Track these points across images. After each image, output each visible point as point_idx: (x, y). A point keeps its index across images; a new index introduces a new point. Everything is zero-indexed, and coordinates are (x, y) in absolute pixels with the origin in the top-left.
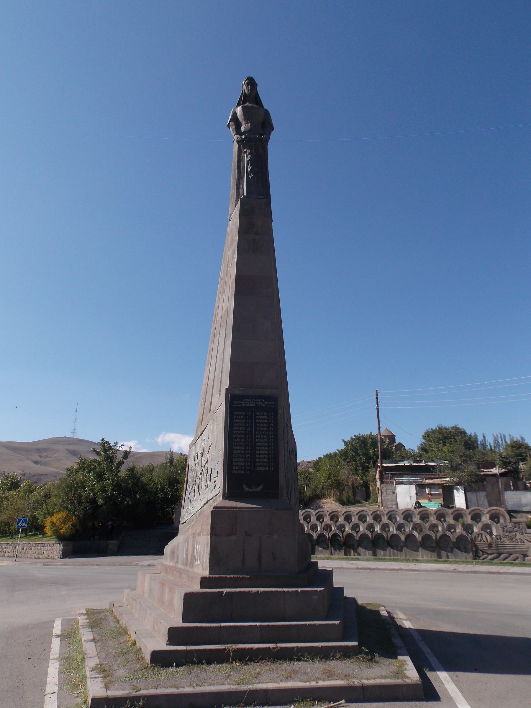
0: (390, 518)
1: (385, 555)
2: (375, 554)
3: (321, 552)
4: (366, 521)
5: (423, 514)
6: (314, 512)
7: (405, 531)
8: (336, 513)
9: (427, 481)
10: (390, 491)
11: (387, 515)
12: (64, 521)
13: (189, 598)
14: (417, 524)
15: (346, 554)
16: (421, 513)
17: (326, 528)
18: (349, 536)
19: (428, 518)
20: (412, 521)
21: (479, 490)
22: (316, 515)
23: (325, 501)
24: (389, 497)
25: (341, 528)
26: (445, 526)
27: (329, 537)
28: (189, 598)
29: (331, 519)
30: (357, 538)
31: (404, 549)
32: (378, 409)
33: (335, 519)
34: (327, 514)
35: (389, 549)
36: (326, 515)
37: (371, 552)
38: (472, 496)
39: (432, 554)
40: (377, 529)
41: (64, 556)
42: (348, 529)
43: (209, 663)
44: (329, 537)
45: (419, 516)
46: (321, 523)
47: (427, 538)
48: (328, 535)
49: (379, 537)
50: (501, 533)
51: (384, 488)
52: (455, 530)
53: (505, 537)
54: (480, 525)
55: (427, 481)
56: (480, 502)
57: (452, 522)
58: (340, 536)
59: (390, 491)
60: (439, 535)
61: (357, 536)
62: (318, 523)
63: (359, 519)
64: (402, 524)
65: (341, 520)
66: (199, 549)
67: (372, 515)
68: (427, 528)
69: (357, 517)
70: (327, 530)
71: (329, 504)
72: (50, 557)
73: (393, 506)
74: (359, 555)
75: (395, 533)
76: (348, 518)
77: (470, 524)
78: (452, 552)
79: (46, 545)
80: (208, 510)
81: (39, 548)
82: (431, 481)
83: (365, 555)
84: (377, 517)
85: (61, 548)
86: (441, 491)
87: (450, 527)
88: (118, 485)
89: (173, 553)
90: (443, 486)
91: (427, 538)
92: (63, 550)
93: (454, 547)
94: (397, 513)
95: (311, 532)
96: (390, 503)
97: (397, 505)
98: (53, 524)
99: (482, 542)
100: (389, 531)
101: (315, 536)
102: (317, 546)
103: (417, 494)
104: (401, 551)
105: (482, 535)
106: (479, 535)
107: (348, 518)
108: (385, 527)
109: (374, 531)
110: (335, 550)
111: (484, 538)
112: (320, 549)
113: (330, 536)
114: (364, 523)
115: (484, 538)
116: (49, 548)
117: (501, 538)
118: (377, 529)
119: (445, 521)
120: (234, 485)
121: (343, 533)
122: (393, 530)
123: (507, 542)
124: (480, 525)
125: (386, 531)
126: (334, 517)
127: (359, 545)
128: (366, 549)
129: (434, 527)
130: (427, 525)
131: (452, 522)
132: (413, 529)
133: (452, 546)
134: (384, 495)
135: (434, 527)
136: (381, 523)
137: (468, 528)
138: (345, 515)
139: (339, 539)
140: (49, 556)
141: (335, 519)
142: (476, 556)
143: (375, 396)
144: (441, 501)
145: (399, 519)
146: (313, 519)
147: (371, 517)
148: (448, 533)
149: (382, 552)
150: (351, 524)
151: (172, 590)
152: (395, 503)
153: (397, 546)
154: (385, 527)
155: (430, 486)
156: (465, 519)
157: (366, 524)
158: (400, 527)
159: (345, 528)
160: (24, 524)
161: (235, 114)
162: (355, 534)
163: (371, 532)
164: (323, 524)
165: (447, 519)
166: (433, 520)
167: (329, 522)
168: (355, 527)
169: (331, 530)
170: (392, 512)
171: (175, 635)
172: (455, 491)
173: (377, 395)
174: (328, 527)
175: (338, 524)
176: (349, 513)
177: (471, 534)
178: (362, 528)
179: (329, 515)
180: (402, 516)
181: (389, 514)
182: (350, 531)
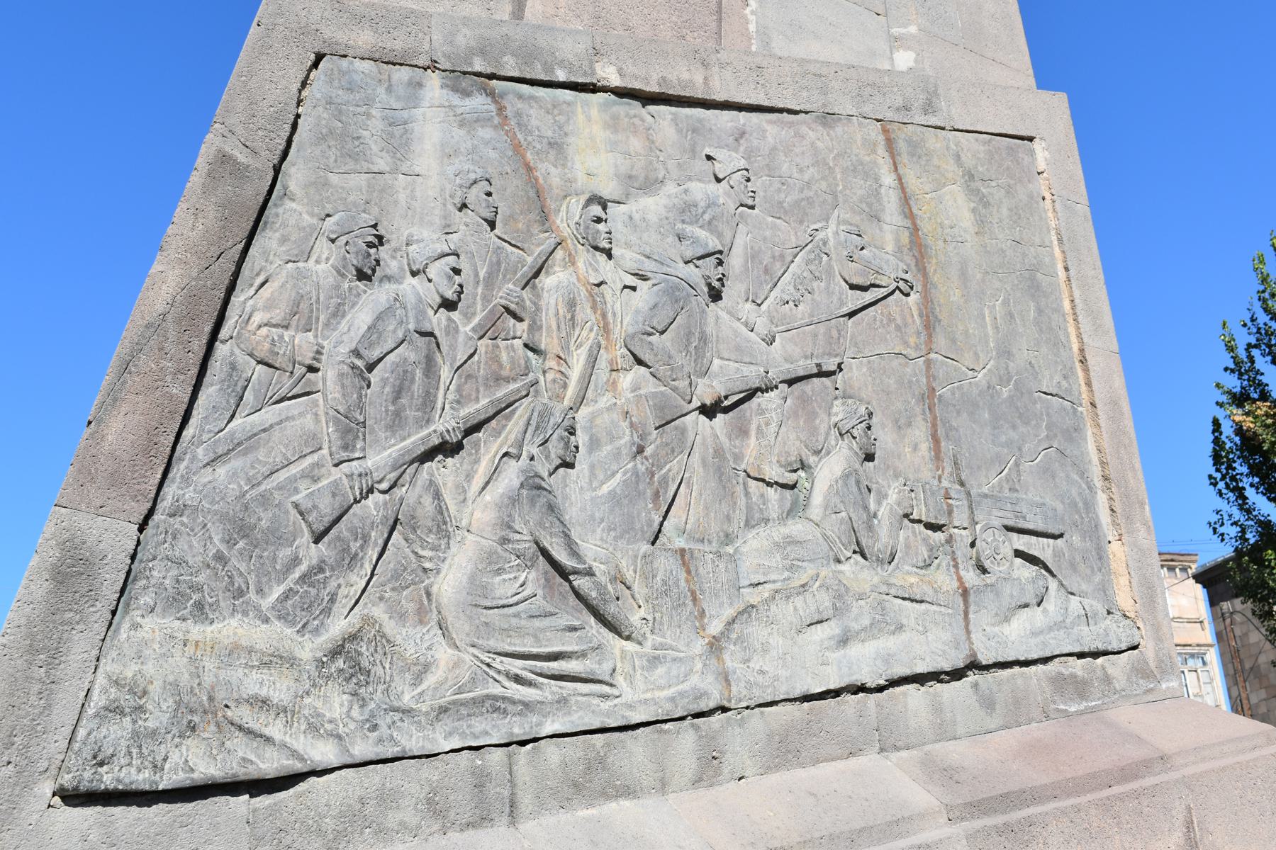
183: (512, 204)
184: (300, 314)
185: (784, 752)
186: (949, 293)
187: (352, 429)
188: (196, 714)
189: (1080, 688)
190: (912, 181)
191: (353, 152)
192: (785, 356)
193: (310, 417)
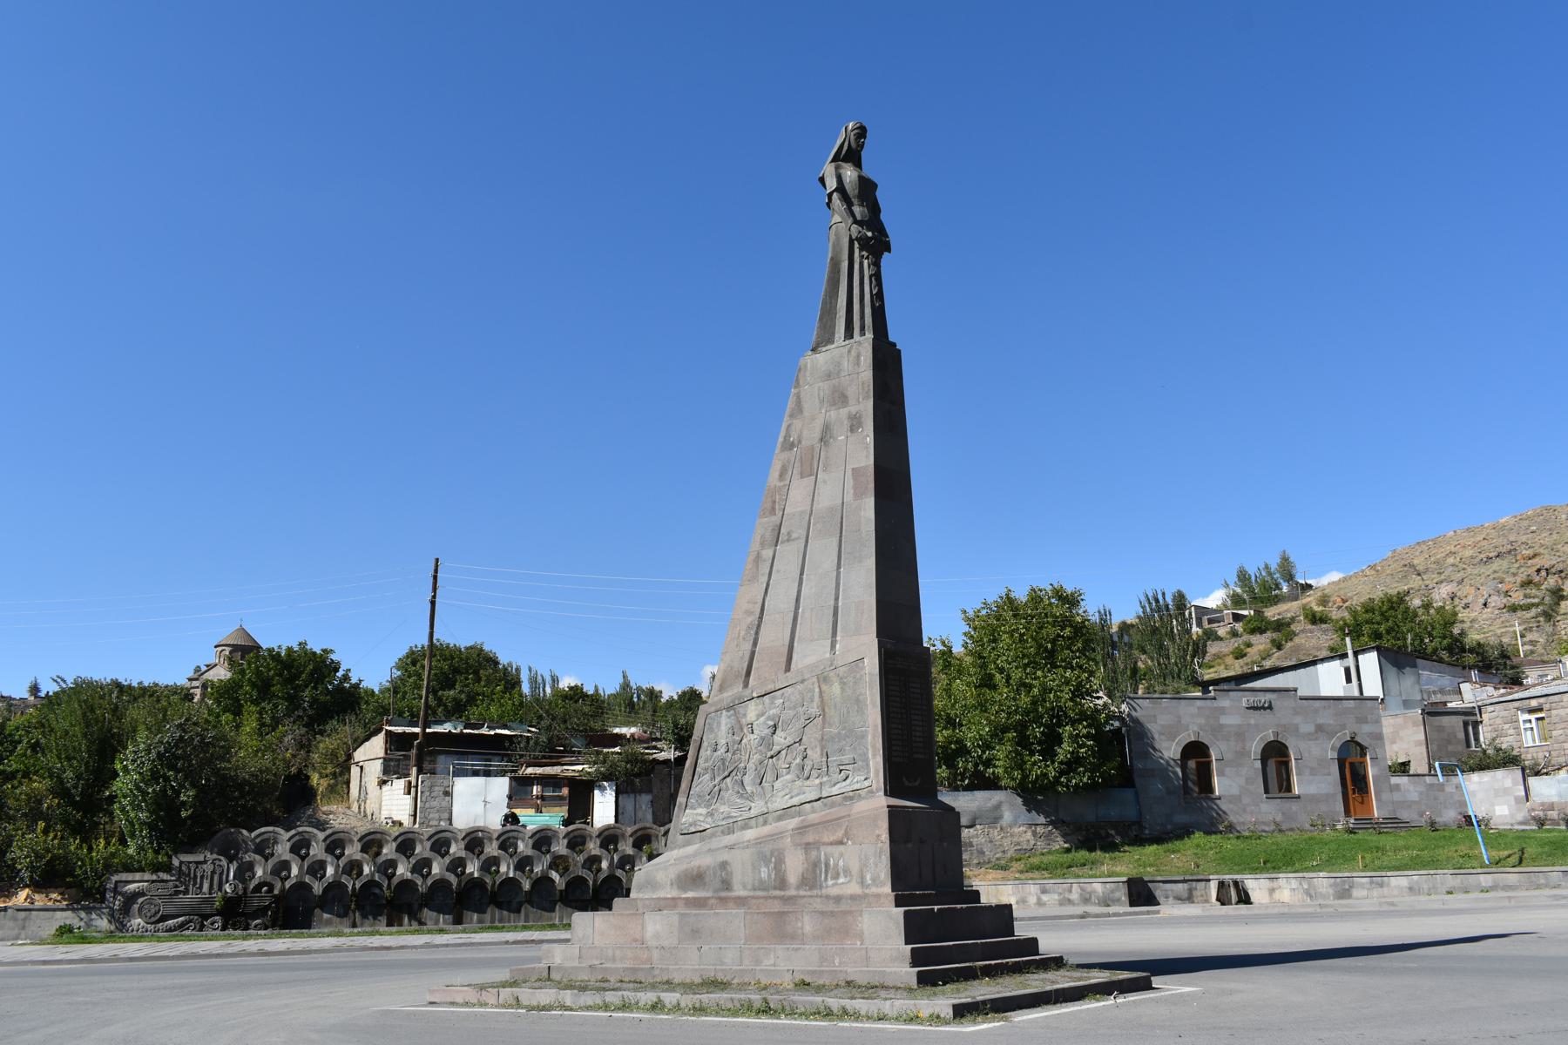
3: (328, 923)
4: (447, 852)
6: (285, 835)
9: (530, 770)
10: (438, 790)
18: (406, 884)
19: (584, 843)
20: (549, 851)
21: (641, 792)
24: (435, 803)
25: (388, 867)
29: (363, 850)
32: (433, 603)
36: (351, 841)
37: (449, 918)
38: (628, 802)
40: (473, 868)
42: (402, 870)
43: (966, 979)
44: (354, 888)
46: (338, 858)
47: (576, 883)
49: (476, 884)
55: (530, 770)
56: (640, 814)
57: (630, 851)
58: (379, 885)
59: (438, 790)
60: (602, 876)
61: (422, 886)
62: (329, 859)
63: (432, 849)
64: (528, 858)
65: (388, 851)
69: (428, 845)
70: (349, 874)
74: (421, 923)
82: (539, 770)
83: (437, 923)
86: (565, 791)
90: (572, 782)
91: (576, 883)
95: (307, 879)
100: (498, 872)
101: (318, 888)
103: (510, 797)
108: (490, 864)
109: (463, 872)
110: (364, 916)
112: (326, 916)
119: (616, 850)
121: (390, 877)
122: (506, 869)
129: (593, 861)
130: (581, 859)
131: (630, 851)
135: (593, 861)
136: (483, 857)
143: (432, 572)
144: (563, 812)
146: (317, 850)
148: (619, 873)
149: (475, 916)
150: (413, 861)
152: (446, 815)
153: (510, 903)
154: (490, 864)
155: (545, 781)
158: (523, 864)
159: (395, 868)
161: (839, 178)
163: (457, 875)
164: (342, 862)
165: (620, 847)
168: (422, 866)
169: (360, 873)
171: (917, 959)
172: (596, 792)
173: (436, 571)
174: (354, 868)
175: (381, 859)
180: (531, 842)
183: (737, 729)
184: (707, 761)
185: (780, 819)
186: (830, 712)
187: (714, 778)
188: (694, 824)
189: (851, 798)
190: (824, 687)
191: (711, 730)
192: (790, 740)
193: (707, 777)
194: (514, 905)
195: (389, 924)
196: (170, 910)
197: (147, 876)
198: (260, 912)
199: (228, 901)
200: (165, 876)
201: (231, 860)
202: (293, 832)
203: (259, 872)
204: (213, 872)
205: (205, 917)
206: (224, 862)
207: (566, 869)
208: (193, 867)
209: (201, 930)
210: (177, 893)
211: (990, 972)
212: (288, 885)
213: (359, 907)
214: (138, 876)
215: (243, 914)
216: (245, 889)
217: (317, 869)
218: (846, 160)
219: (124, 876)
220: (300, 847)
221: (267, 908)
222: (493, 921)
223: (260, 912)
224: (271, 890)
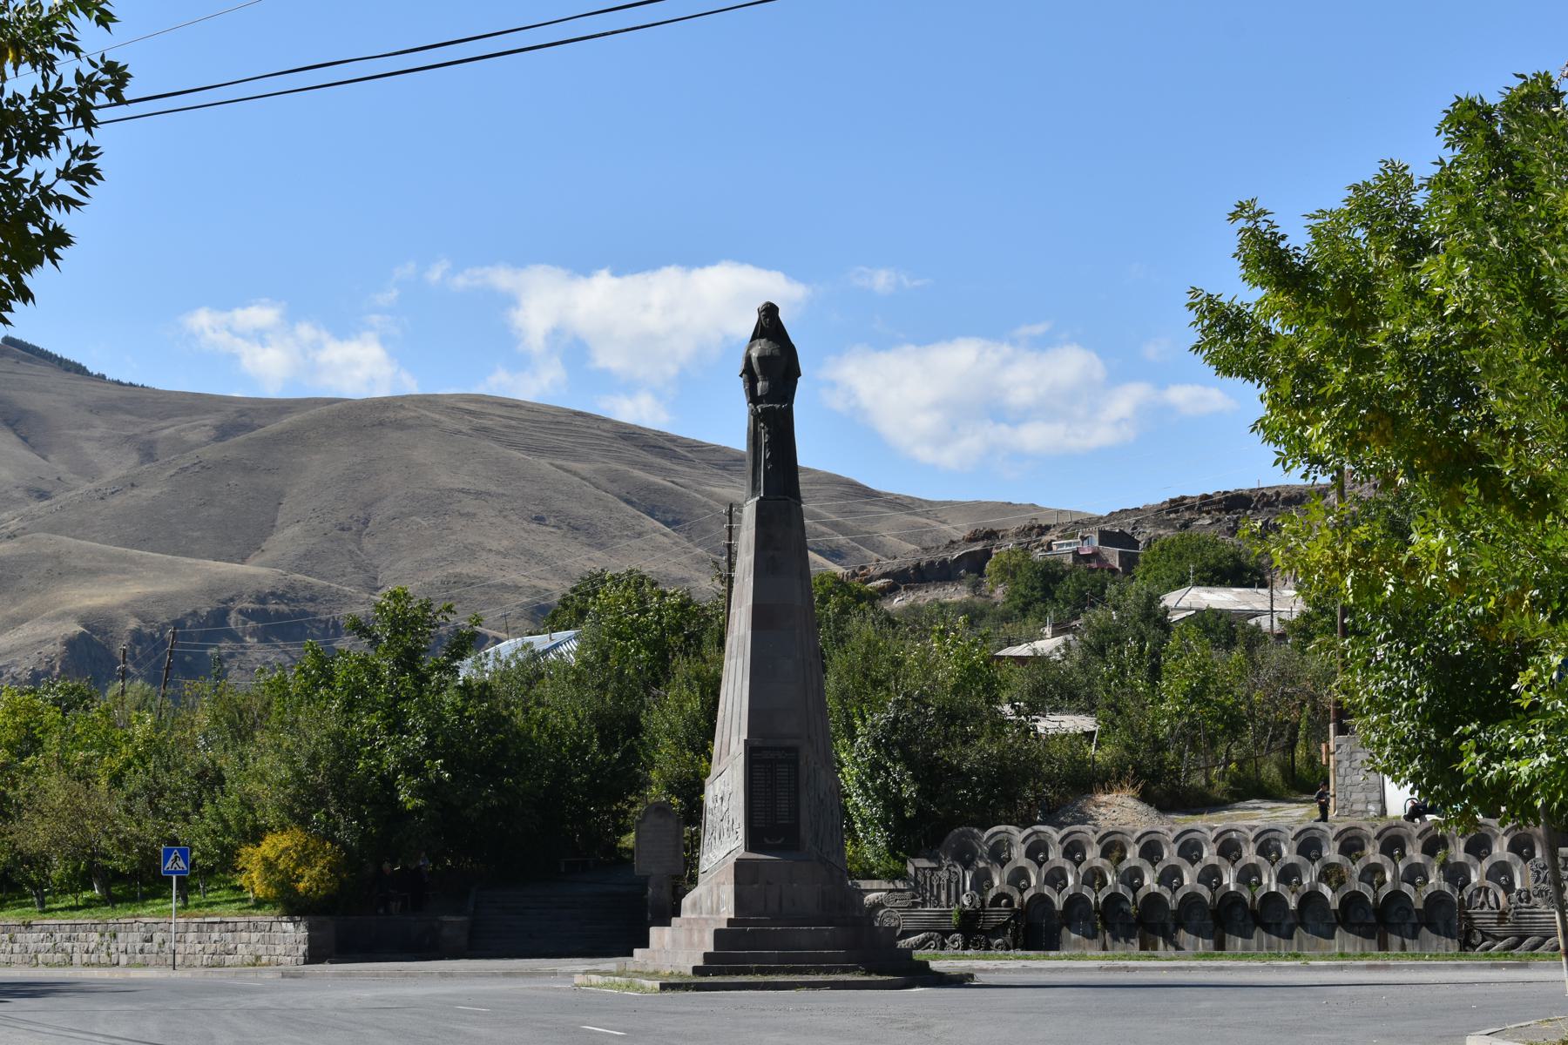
0: (1263, 850)
1: (1245, 948)
2: (1220, 946)
3: (1076, 945)
4: (1200, 857)
5: (1348, 839)
7: (1300, 883)
8: (1119, 837)
11: (1255, 840)
12: (305, 859)
13: (718, 933)
14: (1332, 865)
15: (1143, 948)
16: (1344, 836)
17: (1090, 877)
18: (1153, 898)
19: (1362, 848)
20: (1320, 856)
22: (1061, 842)
23: (1103, 798)
25: (1132, 878)
26: (1401, 868)
27: (1097, 903)
28: (718, 933)
29: (1105, 854)
30: (1173, 905)
31: (1299, 932)
33: (1116, 854)
34: (1095, 839)
35: (1258, 932)
36: (1090, 843)
37: (1210, 943)
39: (1367, 942)
40: (1229, 880)
41: (315, 955)
42: (1150, 881)
44: (1097, 903)
45: (1337, 844)
46: (1078, 864)
47: (1353, 901)
48: (1096, 897)
49: (1232, 900)
50: (1531, 884)
51: (1345, 748)
52: (1426, 880)
53: (1540, 894)
54: (1486, 865)
58: (1125, 899)
60: (1385, 891)
61: (1173, 900)
62: (1068, 865)
63: (1180, 853)
64: (1292, 865)
65: (1133, 855)
66: (724, 897)
67: (1215, 841)
68: (1356, 876)
69: (1175, 848)
70: (1092, 886)
71: (1120, 811)
72: (265, 959)
73: (1371, 807)
74: (1178, 948)
75: (1273, 889)
76: (1190, 850)
77: (1460, 863)
78: (1414, 936)
79: (240, 926)
80: (731, 861)
81: (215, 936)
83: (1196, 947)
84: (1229, 848)
85: (302, 933)
87: (1415, 874)
88: (445, 743)
89: (694, 905)
91: (1353, 901)
92: (311, 940)
93: (1422, 925)
94: (1282, 836)
95: (1047, 890)
96: (1362, 796)
97: (1382, 801)
98: (269, 865)
99: (1486, 909)
101: (1058, 902)
102: (1065, 930)
104: (1290, 937)
105: (1487, 890)
106: (1479, 889)
107: (1151, 850)
108: (1249, 875)
110: (1115, 938)
111: (1491, 898)
112: (1074, 936)
113: (1101, 900)
114: (1193, 863)
115: (1491, 898)
116: (255, 936)
117: (1528, 899)
118: (1229, 880)
119: (1403, 855)
120: (754, 839)
121: (1135, 890)
123: (1543, 908)
124: (1486, 865)
125: (1250, 886)
126: (1113, 847)
127: (1179, 925)
128: (1197, 935)
129: (1372, 873)
130: (1357, 868)
132: (1320, 879)
133: (1415, 920)
134: (1342, 771)
135: (1372, 873)
136: (1239, 864)
137: (1456, 874)
138: (1143, 841)
139: (1125, 907)
140: (258, 958)
141: (1116, 854)
142: (1466, 945)
145: (1289, 854)
146: (1055, 856)
147: (1214, 848)
148: (1406, 888)
149: (1240, 941)
150: (1159, 868)
151: (701, 931)
152: (1376, 796)
153: (1278, 925)
154: (1249, 875)
156: (1452, 849)
157: (1198, 867)
158: (1288, 875)
159: (1142, 879)
160: (181, 863)
162: (1168, 895)
163: (1210, 888)
165: (1409, 851)
166: (1373, 854)
167: (1099, 862)
168: (1170, 876)
169: (1104, 883)
170: (1270, 835)
175: (1124, 866)
176: (1154, 836)
177: (1461, 888)
178: (1189, 877)
179: (1099, 842)
180: (1295, 845)
181: (1261, 840)
182: (1155, 888)
194: (1284, 929)
195: (1143, 948)
196: (909, 925)
197: (885, 885)
198: (999, 930)
199: (964, 915)
200: (900, 885)
201: (966, 867)
202: (1029, 831)
203: (997, 882)
204: (949, 881)
205: (946, 934)
206: (959, 869)
207: (1341, 882)
208: (928, 873)
209: (942, 949)
210: (915, 905)
211: (763, 971)
212: (1027, 895)
213: (1106, 925)
214: (875, 884)
215: (982, 932)
216: (983, 902)
217: (1056, 878)
218: (761, 337)
219: (864, 884)
220: (1036, 850)
221: (1006, 924)
222: (1260, 948)
223: (999, 930)
224: (1010, 903)
